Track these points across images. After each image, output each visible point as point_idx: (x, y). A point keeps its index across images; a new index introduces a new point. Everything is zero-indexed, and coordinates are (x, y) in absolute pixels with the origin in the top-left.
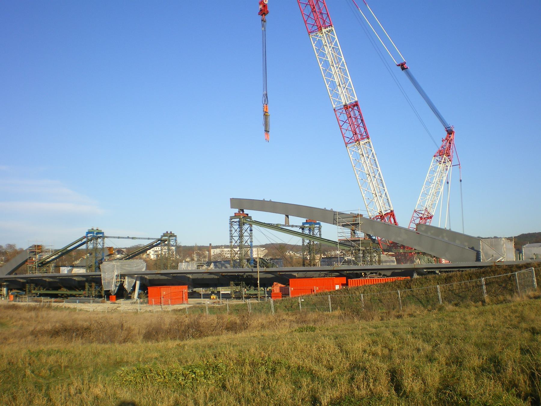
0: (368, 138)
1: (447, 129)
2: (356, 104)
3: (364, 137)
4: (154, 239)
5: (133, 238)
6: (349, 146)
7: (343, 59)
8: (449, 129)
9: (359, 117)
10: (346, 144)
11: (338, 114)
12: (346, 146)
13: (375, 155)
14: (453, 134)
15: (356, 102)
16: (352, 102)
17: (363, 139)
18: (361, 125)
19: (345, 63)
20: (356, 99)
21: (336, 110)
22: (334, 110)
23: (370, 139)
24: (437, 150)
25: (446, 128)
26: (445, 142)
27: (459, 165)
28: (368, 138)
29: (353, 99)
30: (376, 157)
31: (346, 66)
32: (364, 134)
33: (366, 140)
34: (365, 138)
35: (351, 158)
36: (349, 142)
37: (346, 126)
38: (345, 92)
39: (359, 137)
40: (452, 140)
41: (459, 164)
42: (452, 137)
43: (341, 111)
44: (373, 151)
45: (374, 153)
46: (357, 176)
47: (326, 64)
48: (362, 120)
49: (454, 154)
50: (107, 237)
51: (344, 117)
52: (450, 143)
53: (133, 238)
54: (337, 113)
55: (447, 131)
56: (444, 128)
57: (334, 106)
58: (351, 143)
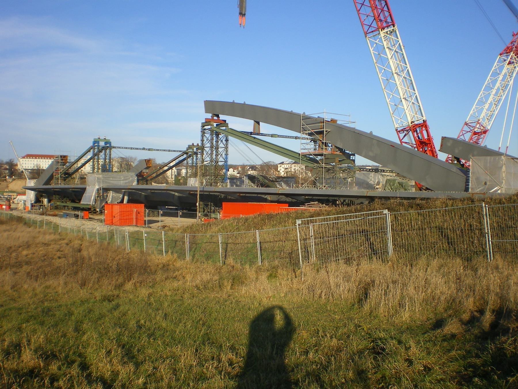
4: (181, 151)
5: (149, 150)
6: (369, 35)
10: (366, 33)
50: (114, 147)
53: (149, 150)
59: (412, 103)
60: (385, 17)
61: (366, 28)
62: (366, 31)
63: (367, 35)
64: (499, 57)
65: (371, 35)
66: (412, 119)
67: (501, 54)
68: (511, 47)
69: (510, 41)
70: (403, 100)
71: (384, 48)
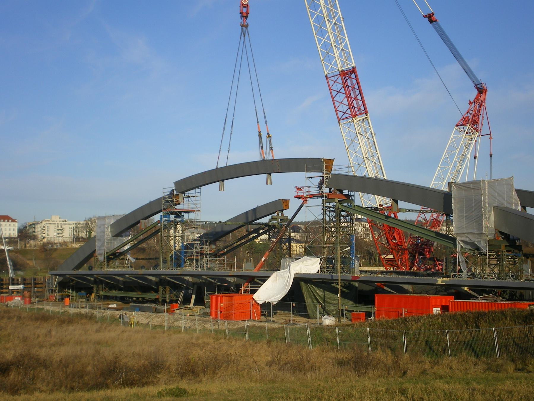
0: (366, 114)
1: (478, 86)
2: (353, 71)
3: (363, 112)
6: (342, 122)
7: (340, 13)
9: (356, 87)
10: (339, 120)
11: (331, 83)
12: (339, 123)
13: (373, 135)
14: (484, 93)
15: (354, 68)
16: (349, 68)
18: (359, 97)
19: (342, 19)
20: (354, 65)
21: (328, 77)
22: (326, 77)
23: (368, 115)
25: (476, 85)
26: (473, 105)
27: (490, 134)
28: (366, 114)
29: (350, 65)
30: (374, 137)
31: (342, 22)
32: (362, 108)
33: (364, 116)
34: (363, 113)
36: (343, 118)
37: (342, 97)
40: (482, 102)
41: (490, 133)
42: (482, 98)
44: (372, 129)
45: (373, 132)
47: (320, 20)
49: (485, 120)
51: (338, 86)
52: (480, 107)
54: (330, 81)
55: (477, 88)
56: (473, 85)
58: (343, 119)
59: (374, 162)
60: (352, 83)
61: (340, 114)
62: (340, 118)
63: (340, 121)
64: (455, 129)
66: (380, 202)
67: (457, 126)
68: (467, 118)
69: (466, 111)
70: (358, 135)
71: (332, 46)
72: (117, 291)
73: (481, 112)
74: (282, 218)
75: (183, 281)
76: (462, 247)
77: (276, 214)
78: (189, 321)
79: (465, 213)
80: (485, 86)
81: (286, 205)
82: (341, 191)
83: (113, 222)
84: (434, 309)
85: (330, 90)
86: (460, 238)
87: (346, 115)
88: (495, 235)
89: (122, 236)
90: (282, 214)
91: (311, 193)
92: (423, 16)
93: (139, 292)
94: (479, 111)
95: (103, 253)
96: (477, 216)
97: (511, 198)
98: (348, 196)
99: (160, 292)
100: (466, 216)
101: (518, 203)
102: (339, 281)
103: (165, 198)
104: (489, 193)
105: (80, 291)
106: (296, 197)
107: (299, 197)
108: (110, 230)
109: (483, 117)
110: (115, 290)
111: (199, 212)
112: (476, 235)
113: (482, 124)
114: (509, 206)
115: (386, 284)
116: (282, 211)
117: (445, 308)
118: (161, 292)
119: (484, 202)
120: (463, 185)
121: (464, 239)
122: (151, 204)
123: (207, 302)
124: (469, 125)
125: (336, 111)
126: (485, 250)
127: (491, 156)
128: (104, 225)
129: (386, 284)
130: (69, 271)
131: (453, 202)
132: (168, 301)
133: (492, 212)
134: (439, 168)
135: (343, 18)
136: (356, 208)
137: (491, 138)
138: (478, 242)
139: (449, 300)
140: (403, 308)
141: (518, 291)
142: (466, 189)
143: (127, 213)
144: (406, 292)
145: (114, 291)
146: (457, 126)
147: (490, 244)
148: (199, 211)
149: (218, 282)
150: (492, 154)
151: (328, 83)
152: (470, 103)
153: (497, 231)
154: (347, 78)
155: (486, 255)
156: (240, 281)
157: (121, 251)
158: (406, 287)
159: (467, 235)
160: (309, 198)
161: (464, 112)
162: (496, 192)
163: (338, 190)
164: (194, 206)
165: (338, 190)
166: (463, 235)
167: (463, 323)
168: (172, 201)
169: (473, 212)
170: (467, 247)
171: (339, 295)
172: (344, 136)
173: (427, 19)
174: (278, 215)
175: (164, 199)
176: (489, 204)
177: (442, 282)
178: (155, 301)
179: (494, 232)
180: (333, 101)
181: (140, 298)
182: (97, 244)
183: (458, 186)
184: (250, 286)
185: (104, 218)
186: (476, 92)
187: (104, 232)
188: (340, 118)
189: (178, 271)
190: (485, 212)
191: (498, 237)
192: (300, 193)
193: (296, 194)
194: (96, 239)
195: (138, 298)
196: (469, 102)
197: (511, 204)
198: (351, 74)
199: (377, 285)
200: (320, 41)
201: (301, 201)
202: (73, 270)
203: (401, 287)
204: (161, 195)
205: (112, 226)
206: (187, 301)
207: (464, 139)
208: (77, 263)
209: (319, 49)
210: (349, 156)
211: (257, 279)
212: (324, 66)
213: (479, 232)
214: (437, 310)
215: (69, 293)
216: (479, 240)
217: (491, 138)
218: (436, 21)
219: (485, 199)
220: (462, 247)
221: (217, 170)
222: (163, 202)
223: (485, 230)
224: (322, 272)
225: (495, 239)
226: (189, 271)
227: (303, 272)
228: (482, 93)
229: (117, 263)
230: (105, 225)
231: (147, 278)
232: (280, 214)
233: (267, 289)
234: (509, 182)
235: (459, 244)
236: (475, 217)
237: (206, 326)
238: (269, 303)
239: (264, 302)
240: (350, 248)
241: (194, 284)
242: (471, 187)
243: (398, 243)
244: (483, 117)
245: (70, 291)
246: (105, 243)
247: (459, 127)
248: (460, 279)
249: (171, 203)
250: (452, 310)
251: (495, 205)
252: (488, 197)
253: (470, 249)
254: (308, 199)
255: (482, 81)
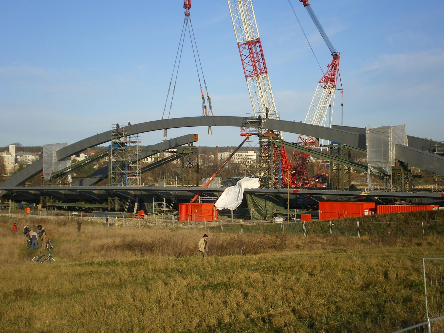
1: (334, 54)
2: (258, 41)
3: (263, 71)
8: (335, 54)
10: (247, 77)
11: (241, 49)
12: (246, 79)
13: (271, 89)
14: (338, 59)
17: (262, 73)
18: (261, 61)
20: (259, 37)
21: (240, 44)
22: (238, 44)
24: (323, 75)
25: (332, 53)
27: (342, 89)
28: (266, 72)
30: (271, 90)
31: (252, 4)
33: (264, 75)
35: (249, 89)
37: (247, 60)
38: (249, 30)
39: (259, 71)
40: (337, 65)
42: (337, 63)
43: (243, 46)
44: (270, 85)
45: (270, 87)
46: (254, 107)
48: (262, 57)
49: (338, 80)
51: (246, 52)
52: (335, 69)
55: (333, 56)
57: (238, 42)
65: (250, 78)
72: (60, 202)
73: (336, 73)
74: (192, 148)
75: (129, 194)
76: (371, 170)
77: (187, 145)
78: (160, 223)
79: (376, 148)
80: (339, 55)
81: (195, 139)
82: (272, 131)
83: (58, 150)
84: (365, 211)
85: (241, 54)
86: (371, 165)
87: (252, 74)
88: (395, 163)
89: (65, 160)
90: (192, 145)
91: (251, 132)
92: (300, 1)
93: (87, 203)
94: (335, 72)
95: (51, 173)
96: (385, 150)
97: (404, 138)
98: (277, 135)
99: (109, 203)
100: (376, 151)
101: (407, 142)
102: (288, 193)
103: (113, 132)
104: (392, 135)
105: (20, 203)
106: (241, 135)
107: (243, 135)
108: (56, 156)
109: (337, 77)
110: (59, 202)
111: (140, 143)
112: (383, 163)
113: (337, 82)
114: (401, 143)
115: (313, 195)
116: (192, 142)
117: (371, 210)
118: (110, 203)
119: (391, 142)
120: (375, 130)
121: (374, 165)
122: (98, 136)
123: (154, 209)
124: (329, 82)
125: (245, 70)
126: (390, 173)
127: (342, 105)
128: (51, 151)
129: (313, 195)
130: (13, 187)
131: (367, 141)
132: (109, 209)
133: (394, 148)
134: (308, 113)
135: (252, 2)
136: (283, 142)
137: (342, 92)
138: (385, 167)
139: (372, 205)
140: (344, 211)
141: (408, 199)
142: (377, 132)
143: (70, 143)
144: (323, 200)
145: (57, 203)
146: (319, 82)
147: (393, 169)
148: (140, 142)
149: (166, 195)
150: (343, 103)
151: (239, 49)
152: (328, 66)
153: (397, 161)
154: (253, 46)
155: (390, 176)
156: (192, 194)
157: (65, 172)
158: (323, 197)
159: (376, 163)
160: (250, 136)
161: (325, 72)
162: (396, 135)
163: (270, 130)
164: (135, 138)
165: (270, 130)
166: (373, 163)
167: (421, 217)
168: (122, 134)
169: (381, 148)
170: (375, 171)
171: (288, 203)
172: (249, 88)
173: (302, 3)
174: (189, 145)
175: (113, 133)
176: (392, 143)
177: (365, 193)
178: (105, 209)
179: (395, 161)
180: (243, 63)
181: (83, 207)
182: (43, 166)
183: (372, 131)
184: (203, 197)
185: (52, 145)
186: (332, 58)
187: (51, 157)
188: (247, 75)
189: (123, 187)
190: (391, 148)
191: (397, 164)
192: (244, 133)
193: (241, 133)
194: (43, 162)
195: (80, 208)
196: (328, 65)
197: (404, 142)
198: (256, 43)
199: (307, 196)
200: (234, 17)
201: (244, 138)
202: (16, 186)
203: (321, 197)
204: (111, 129)
205: (59, 152)
206: (131, 210)
207: (325, 92)
208: (21, 180)
209: (234, 24)
210: (252, 103)
211: (204, 193)
212: (237, 37)
213: (386, 161)
214: (366, 212)
215: (9, 204)
216: (385, 166)
217: (342, 92)
218: (309, 5)
219: (391, 139)
220: (371, 170)
221: (294, 123)
222: (112, 135)
223: (391, 160)
224: (260, 187)
225: (395, 165)
226: (131, 187)
227: (249, 187)
228: (337, 59)
229: (59, 181)
230: (53, 151)
231: (29, 193)
232: (191, 145)
233: (222, 199)
234: (402, 128)
235: (370, 168)
236: (383, 151)
237: (179, 225)
238: (227, 209)
239: (223, 208)
240: (295, 171)
241: (135, 196)
242: (381, 131)
243: (285, 167)
244: (337, 77)
245: (10, 203)
246: (53, 166)
247: (321, 83)
248: (391, 192)
249: (121, 136)
250: (379, 211)
251: (395, 143)
252: (392, 138)
253: (377, 172)
254: (249, 136)
255: (337, 51)
